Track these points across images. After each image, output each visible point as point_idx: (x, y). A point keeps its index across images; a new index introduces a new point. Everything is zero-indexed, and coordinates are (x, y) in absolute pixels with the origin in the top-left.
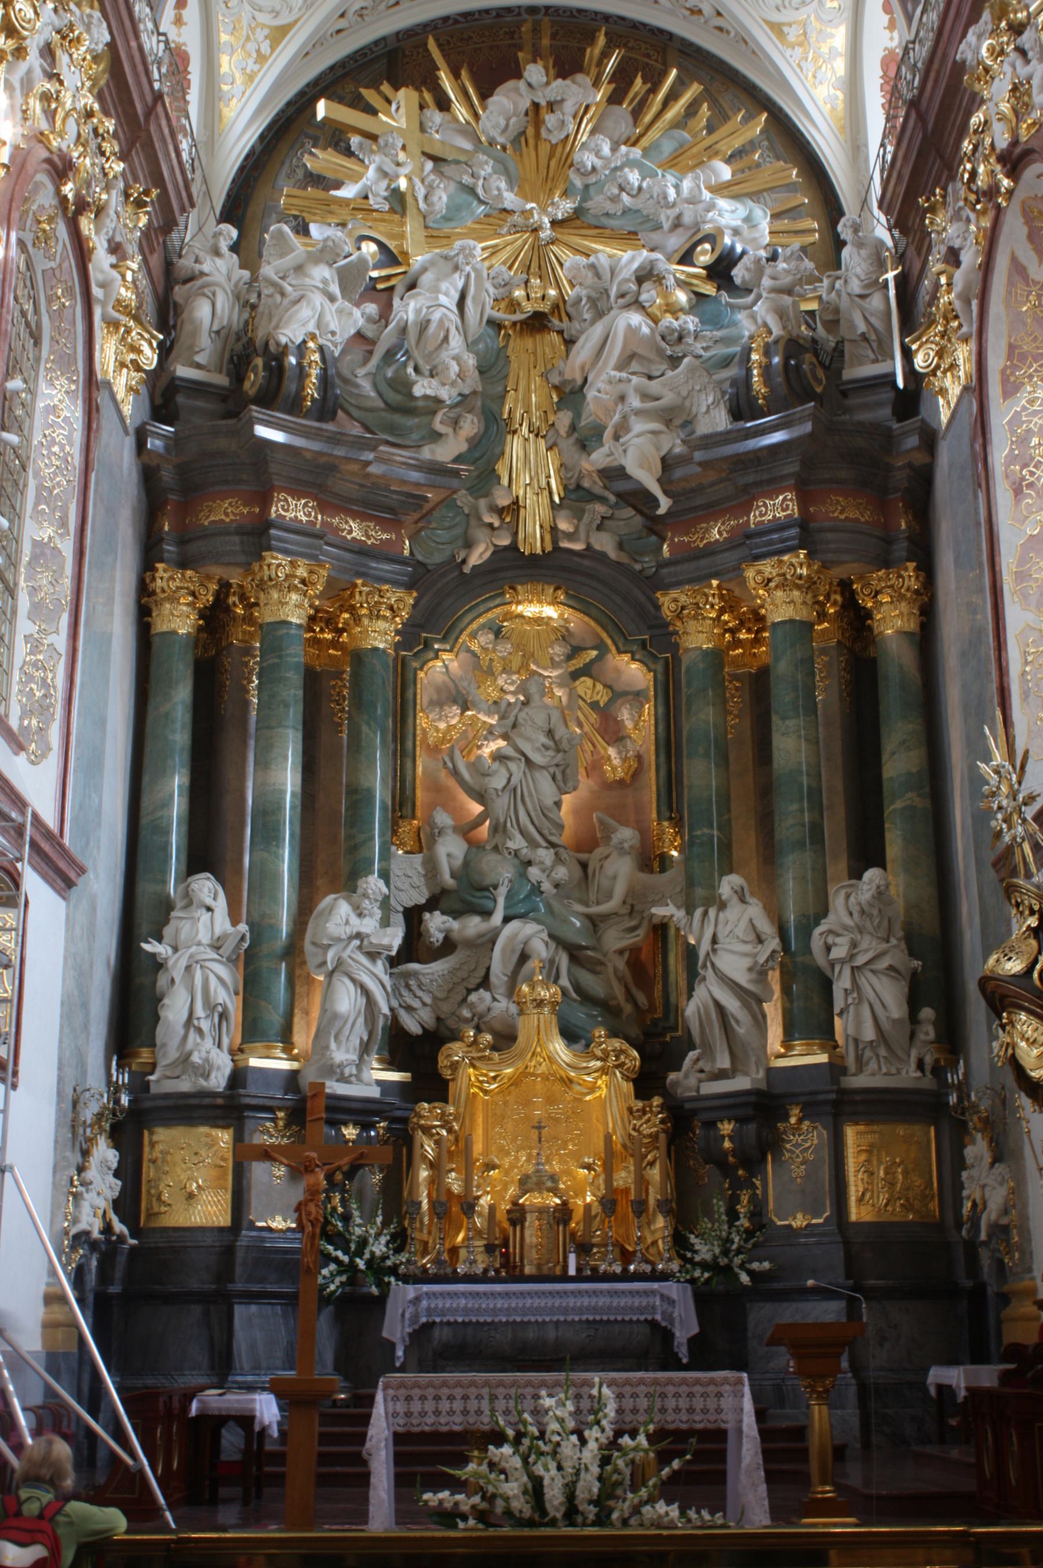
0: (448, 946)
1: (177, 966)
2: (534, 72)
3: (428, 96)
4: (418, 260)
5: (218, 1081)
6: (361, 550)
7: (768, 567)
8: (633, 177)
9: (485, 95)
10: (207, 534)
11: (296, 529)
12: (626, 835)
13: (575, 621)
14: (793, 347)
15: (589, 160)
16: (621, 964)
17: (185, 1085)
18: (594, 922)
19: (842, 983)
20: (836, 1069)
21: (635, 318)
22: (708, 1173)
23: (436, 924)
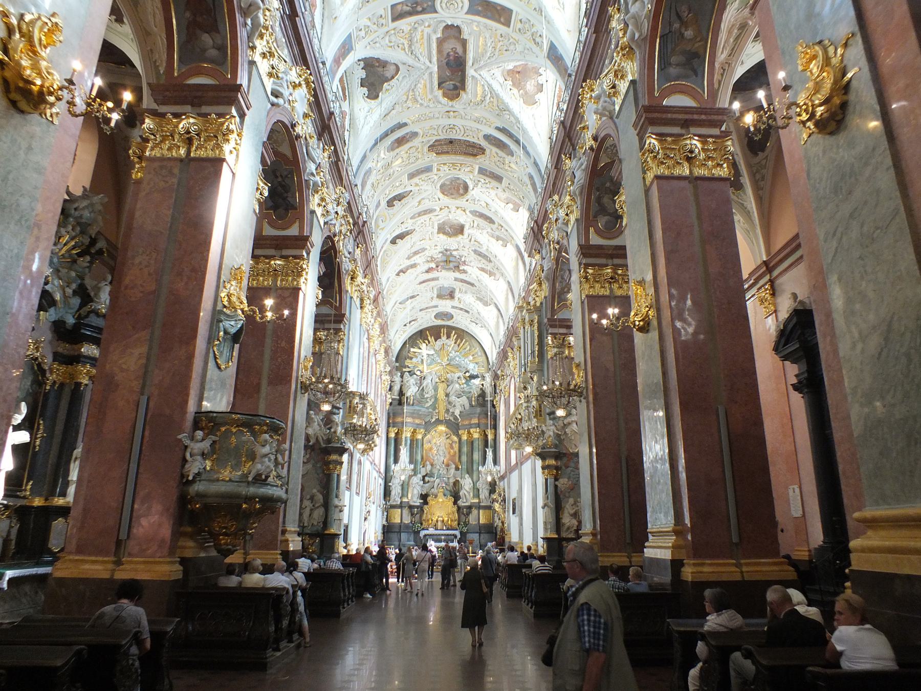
0: (428, 482)
1: (393, 487)
2: (444, 338)
3: (426, 341)
4: (425, 371)
5: (399, 503)
6: (418, 424)
7: (474, 430)
8: (457, 359)
9: (436, 341)
10: (396, 423)
11: (409, 422)
12: (454, 466)
13: (447, 430)
14: (479, 396)
15: (451, 355)
16: (452, 484)
17: (394, 503)
18: (448, 478)
19: (480, 491)
20: (479, 502)
21: (457, 386)
22: (462, 516)
23: (427, 479)
